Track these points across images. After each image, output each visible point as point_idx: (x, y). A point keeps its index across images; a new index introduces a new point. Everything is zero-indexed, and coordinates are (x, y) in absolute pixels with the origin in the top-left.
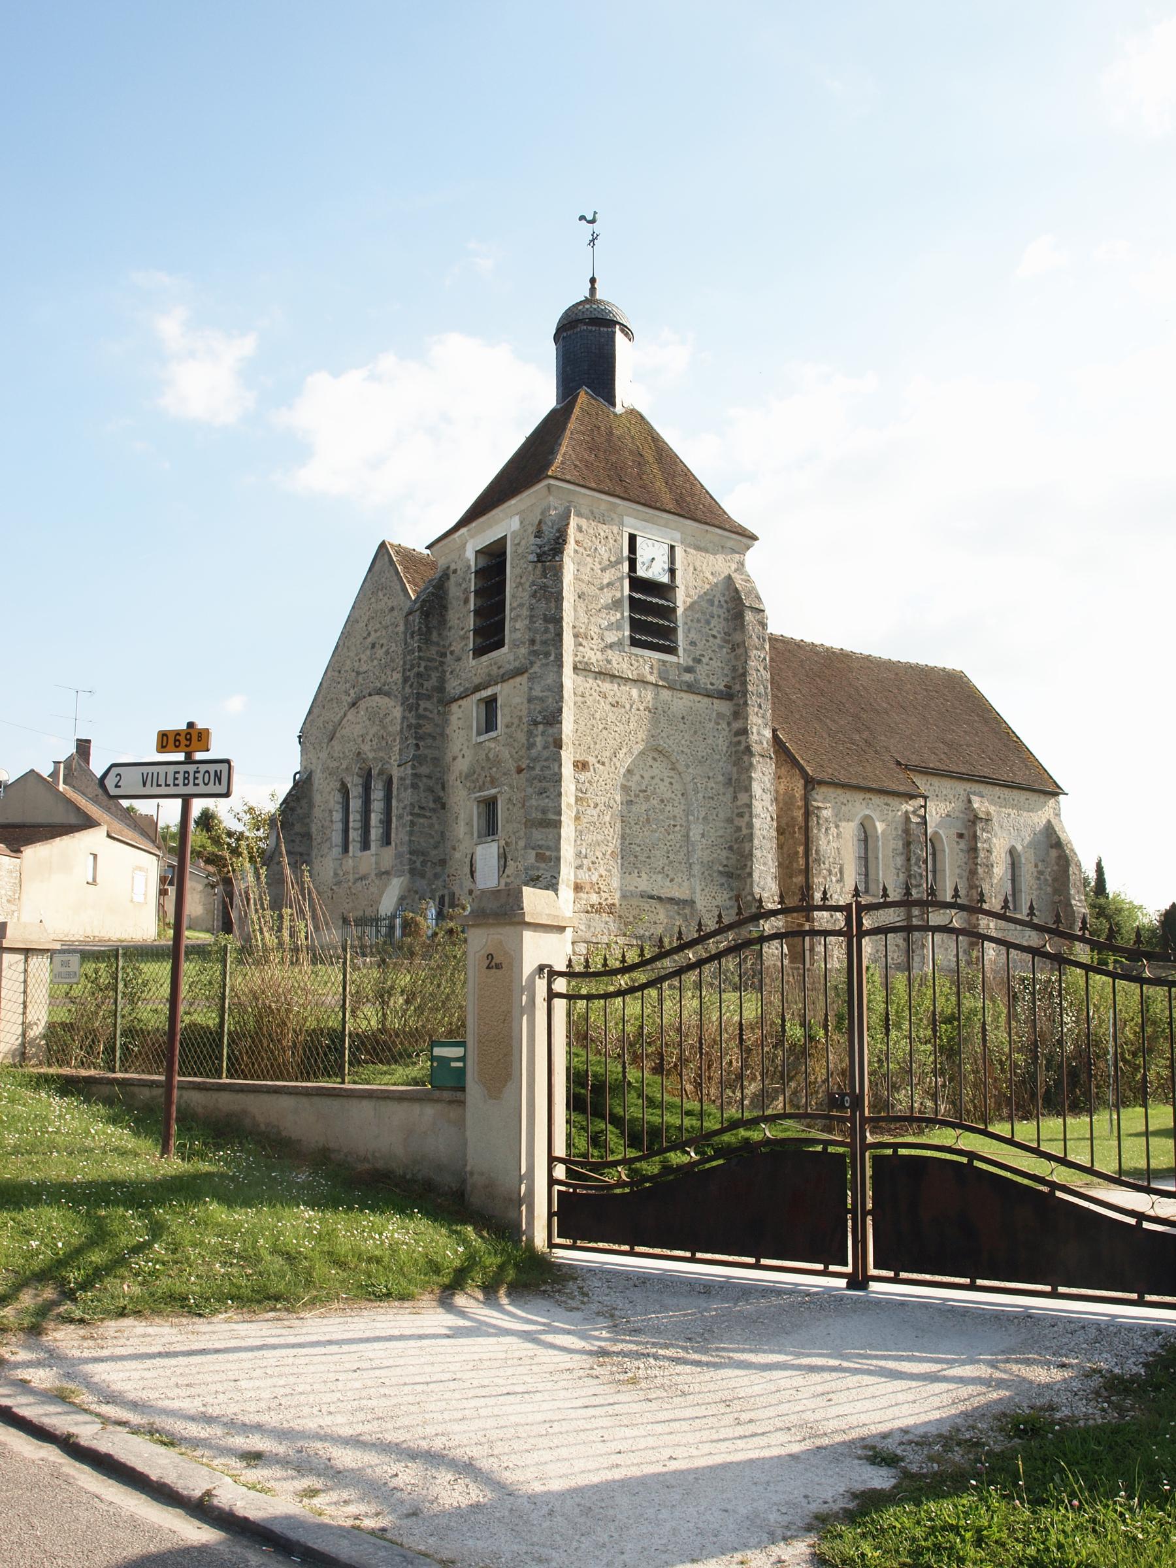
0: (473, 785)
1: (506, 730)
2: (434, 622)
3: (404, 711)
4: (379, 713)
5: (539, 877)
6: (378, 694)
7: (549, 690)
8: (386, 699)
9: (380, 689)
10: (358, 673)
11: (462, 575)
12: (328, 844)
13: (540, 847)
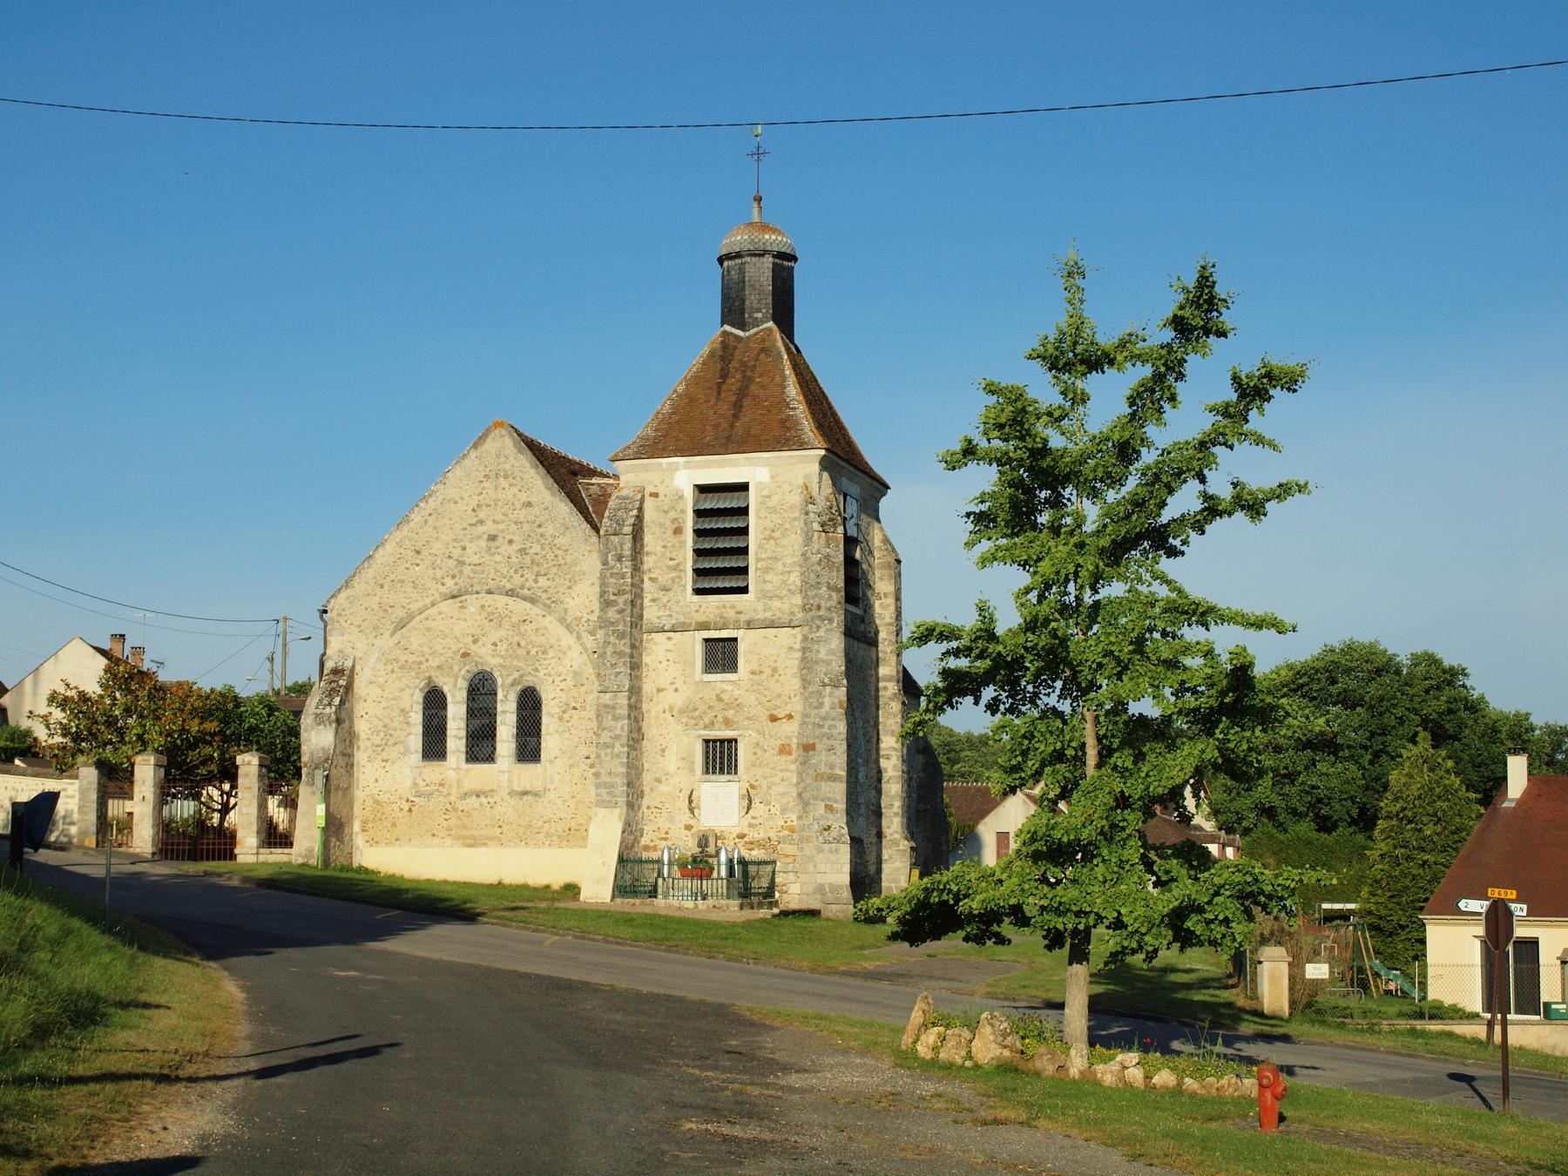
0: (693, 722)
1: (753, 676)
2: (639, 546)
3: (607, 635)
5: (829, 827)
6: (507, 594)
7: (834, 654)
8: (528, 605)
9: (511, 590)
10: (461, 563)
12: (400, 748)
13: (829, 799)
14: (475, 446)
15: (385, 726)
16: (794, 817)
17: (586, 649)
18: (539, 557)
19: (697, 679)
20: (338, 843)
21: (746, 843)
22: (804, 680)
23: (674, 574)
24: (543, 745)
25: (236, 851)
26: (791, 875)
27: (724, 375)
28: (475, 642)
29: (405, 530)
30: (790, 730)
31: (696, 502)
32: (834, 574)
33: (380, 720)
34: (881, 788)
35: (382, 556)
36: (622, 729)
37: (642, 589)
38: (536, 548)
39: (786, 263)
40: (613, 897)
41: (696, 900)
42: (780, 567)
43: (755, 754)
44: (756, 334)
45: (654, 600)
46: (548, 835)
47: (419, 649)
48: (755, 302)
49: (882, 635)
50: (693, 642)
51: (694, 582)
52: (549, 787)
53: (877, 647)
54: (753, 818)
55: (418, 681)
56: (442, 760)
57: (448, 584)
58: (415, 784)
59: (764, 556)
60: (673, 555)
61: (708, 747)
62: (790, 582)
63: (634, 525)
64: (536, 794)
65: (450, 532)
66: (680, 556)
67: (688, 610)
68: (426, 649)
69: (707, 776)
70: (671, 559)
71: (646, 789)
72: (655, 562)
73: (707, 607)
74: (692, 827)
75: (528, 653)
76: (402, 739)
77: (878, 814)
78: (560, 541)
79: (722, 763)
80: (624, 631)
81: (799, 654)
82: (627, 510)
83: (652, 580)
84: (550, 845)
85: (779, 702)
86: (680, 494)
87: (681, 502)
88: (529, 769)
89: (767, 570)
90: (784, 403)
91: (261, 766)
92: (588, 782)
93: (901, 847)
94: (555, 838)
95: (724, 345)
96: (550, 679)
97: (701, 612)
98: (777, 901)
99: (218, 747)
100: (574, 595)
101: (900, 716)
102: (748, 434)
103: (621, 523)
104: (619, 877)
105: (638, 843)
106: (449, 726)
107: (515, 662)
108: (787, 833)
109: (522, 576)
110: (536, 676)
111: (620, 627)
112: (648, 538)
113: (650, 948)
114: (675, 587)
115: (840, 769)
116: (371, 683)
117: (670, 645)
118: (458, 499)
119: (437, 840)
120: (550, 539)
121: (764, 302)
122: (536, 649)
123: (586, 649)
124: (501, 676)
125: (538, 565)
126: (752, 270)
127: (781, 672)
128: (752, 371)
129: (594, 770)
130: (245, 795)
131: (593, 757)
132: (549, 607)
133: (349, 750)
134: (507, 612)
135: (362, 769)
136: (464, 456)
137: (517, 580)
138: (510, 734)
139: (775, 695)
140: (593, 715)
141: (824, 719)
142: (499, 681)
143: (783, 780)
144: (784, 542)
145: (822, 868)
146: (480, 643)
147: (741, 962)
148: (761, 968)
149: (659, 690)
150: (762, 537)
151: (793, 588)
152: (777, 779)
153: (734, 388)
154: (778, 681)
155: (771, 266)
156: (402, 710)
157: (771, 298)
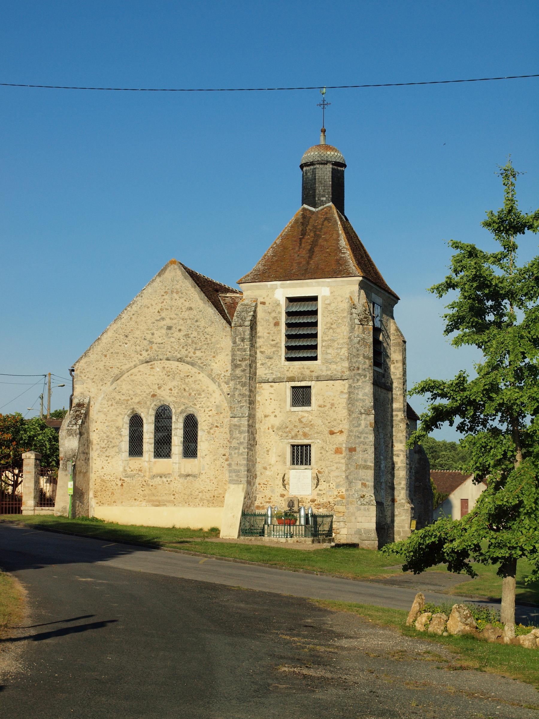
0: (285, 435)
3: (236, 384)
4: (180, 374)
5: (364, 496)
6: (178, 361)
7: (367, 396)
8: (190, 367)
9: (180, 358)
10: (151, 342)
11: (270, 307)
12: (116, 449)
14: (159, 275)
15: (107, 437)
16: (344, 490)
17: (223, 392)
18: (196, 339)
19: (288, 410)
20: (80, 504)
21: (316, 505)
22: (350, 410)
23: (274, 349)
24: (199, 448)
25: (22, 508)
26: (342, 524)
27: (304, 233)
28: (159, 388)
29: (119, 324)
30: (341, 439)
31: (287, 307)
32: (367, 349)
34: (394, 473)
35: (106, 338)
36: (244, 439)
37: (256, 358)
38: (195, 334)
39: (339, 168)
40: (239, 536)
41: (287, 537)
42: (335, 345)
43: (321, 453)
44: (323, 209)
45: (262, 364)
46: (202, 499)
47: (127, 392)
48: (322, 191)
49: (395, 385)
50: (286, 388)
51: (286, 353)
53: (392, 391)
54: (320, 490)
55: (126, 411)
56: (140, 456)
58: (125, 470)
59: (326, 339)
60: (274, 338)
61: (294, 449)
63: (251, 320)
64: (195, 476)
65: (145, 325)
66: (277, 339)
67: (283, 370)
68: (131, 392)
69: (293, 466)
70: (273, 340)
71: (258, 473)
74: (285, 495)
75: (190, 394)
76: (118, 444)
77: (392, 488)
78: (209, 330)
79: (302, 459)
80: (246, 382)
82: (247, 312)
83: (262, 352)
84: (202, 505)
85: (335, 423)
86: (278, 303)
87: (279, 307)
89: (328, 347)
90: (338, 250)
91: (36, 459)
93: (406, 508)
94: (205, 501)
95: (304, 216)
96: (203, 410)
98: (334, 539)
99: (13, 449)
100: (217, 361)
101: (405, 431)
102: (317, 268)
103: (243, 319)
104: (242, 524)
105: (254, 504)
107: (183, 400)
108: (339, 499)
109: (186, 350)
110: (195, 409)
111: (243, 380)
112: (260, 328)
113: (260, 565)
114: (275, 357)
115: (371, 462)
116: (99, 412)
117: (272, 390)
118: (149, 305)
119: (137, 503)
120: (203, 329)
121: (327, 191)
122: (195, 392)
123: (223, 392)
124: (175, 407)
125: (196, 344)
128: (320, 231)
129: (228, 462)
130: (27, 476)
131: (227, 454)
132: (202, 368)
133: (87, 451)
134: (178, 371)
135: (95, 462)
136: (153, 281)
137: (184, 352)
138: (180, 442)
139: (332, 419)
140: (227, 430)
141: (361, 433)
142: (173, 411)
143: (337, 468)
144: (338, 330)
145: (359, 519)
146: (162, 389)
147: (313, 573)
148: (324, 577)
150: (325, 327)
151: (343, 357)
152: (334, 468)
153: (309, 241)
154: (334, 411)
155: (331, 170)
156: (117, 428)
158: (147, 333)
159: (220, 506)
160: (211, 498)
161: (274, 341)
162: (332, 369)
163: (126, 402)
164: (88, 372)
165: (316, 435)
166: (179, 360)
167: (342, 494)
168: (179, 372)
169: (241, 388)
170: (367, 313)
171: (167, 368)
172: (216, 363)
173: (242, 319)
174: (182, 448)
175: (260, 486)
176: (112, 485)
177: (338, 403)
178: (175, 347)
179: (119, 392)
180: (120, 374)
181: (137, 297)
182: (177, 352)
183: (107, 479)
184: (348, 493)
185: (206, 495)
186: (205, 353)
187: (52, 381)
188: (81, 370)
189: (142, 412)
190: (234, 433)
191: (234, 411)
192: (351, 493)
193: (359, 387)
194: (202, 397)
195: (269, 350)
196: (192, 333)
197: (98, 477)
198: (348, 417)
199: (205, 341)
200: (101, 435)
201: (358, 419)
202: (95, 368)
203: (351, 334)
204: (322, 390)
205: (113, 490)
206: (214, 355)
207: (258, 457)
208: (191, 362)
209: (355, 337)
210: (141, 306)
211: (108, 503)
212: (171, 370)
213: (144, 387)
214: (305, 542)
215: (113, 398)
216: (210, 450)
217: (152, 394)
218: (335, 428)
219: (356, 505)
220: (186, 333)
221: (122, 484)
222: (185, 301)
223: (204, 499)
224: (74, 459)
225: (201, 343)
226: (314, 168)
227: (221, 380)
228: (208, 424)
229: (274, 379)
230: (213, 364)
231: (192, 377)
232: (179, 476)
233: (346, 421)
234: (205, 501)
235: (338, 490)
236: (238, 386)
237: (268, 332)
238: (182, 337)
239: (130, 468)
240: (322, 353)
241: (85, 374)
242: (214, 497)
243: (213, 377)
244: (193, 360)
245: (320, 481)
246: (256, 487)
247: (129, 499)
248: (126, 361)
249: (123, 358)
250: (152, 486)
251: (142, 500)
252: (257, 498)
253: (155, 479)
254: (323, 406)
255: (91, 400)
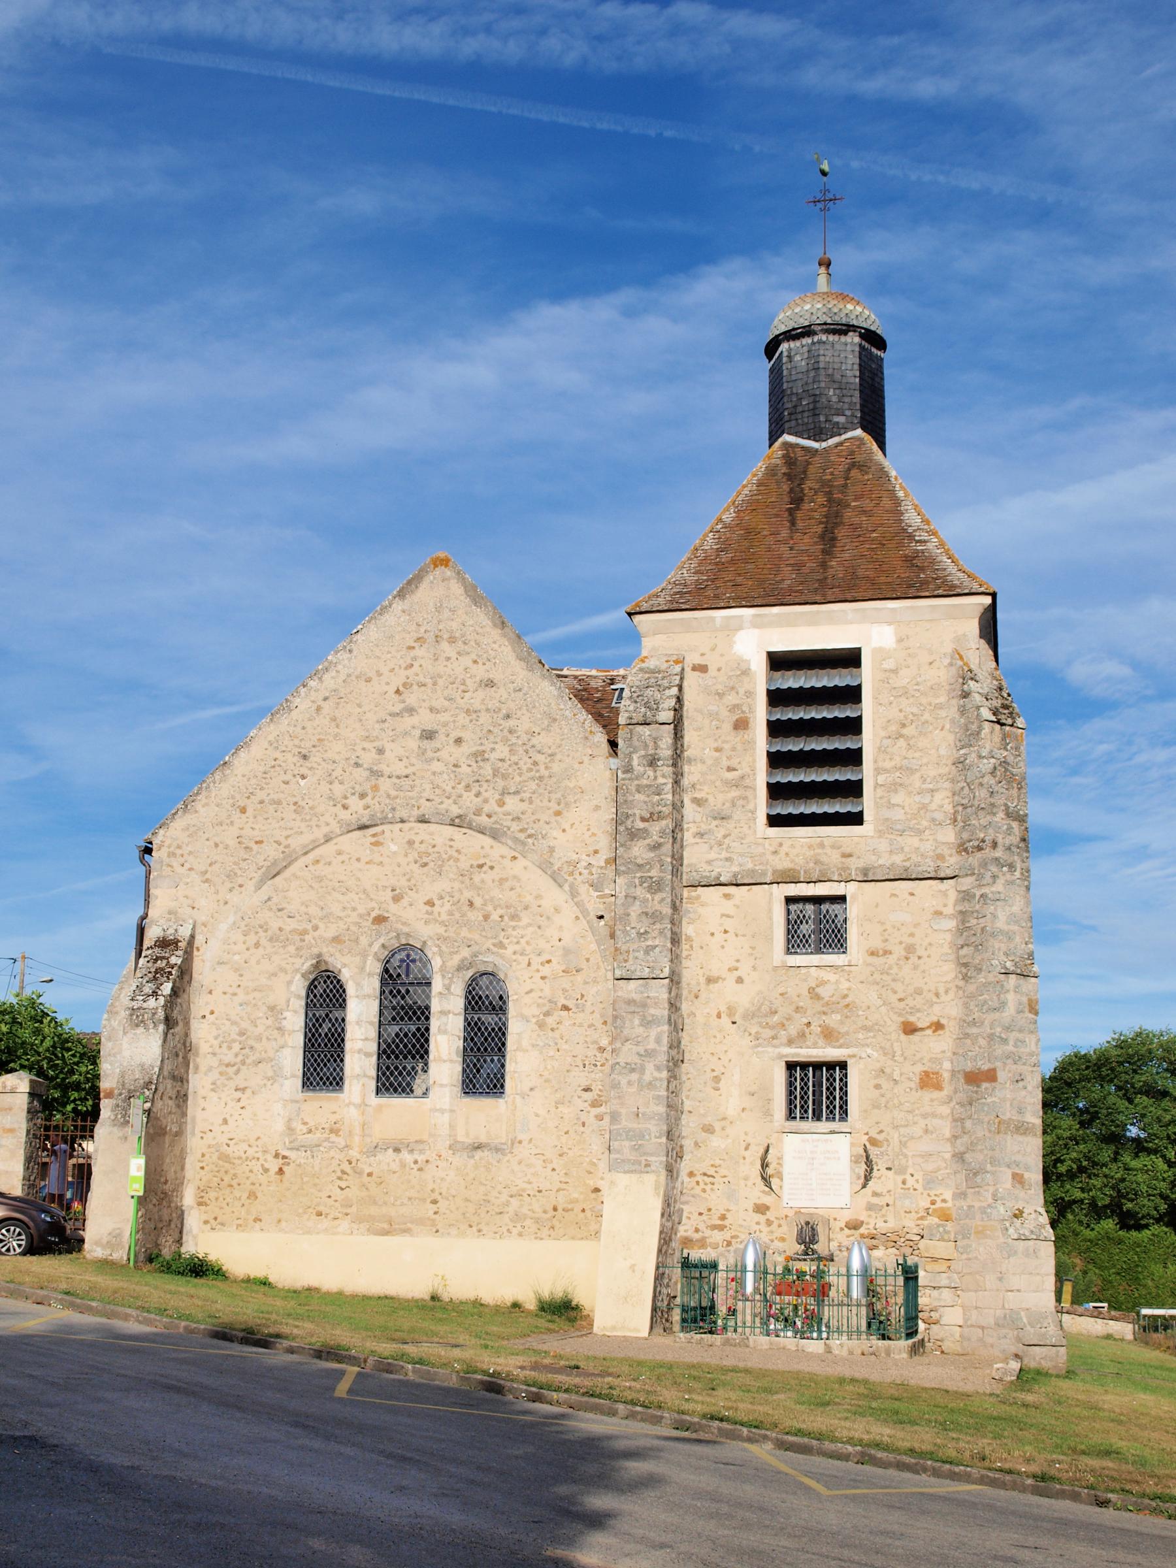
0: (768, 1033)
7: (1017, 922)
8: (487, 841)
9: (459, 817)
10: (376, 773)
14: (401, 594)
15: (242, 1034)
16: (948, 1195)
17: (585, 912)
18: (506, 765)
21: (862, 1236)
23: (734, 793)
24: (509, 1067)
27: (797, 500)
28: (397, 899)
29: (284, 722)
33: (234, 1023)
35: (245, 763)
36: (658, 1041)
38: (502, 751)
39: (874, 350)
43: (877, 1087)
44: (841, 444)
45: (701, 835)
46: (518, 1217)
47: (303, 909)
48: (834, 399)
50: (770, 902)
52: (520, 1137)
54: (875, 1194)
55: (299, 961)
56: (334, 1090)
57: (353, 808)
58: (290, 1130)
59: (888, 765)
60: (734, 763)
62: (933, 806)
67: (760, 850)
68: (313, 910)
70: (730, 769)
72: (703, 774)
73: (792, 846)
74: (768, 1208)
75: (486, 917)
76: (271, 1054)
79: (817, 1103)
80: (662, 879)
81: (952, 924)
82: (661, 689)
83: (698, 802)
84: (520, 1235)
85: (918, 1001)
86: (743, 666)
87: (746, 679)
88: (485, 1104)
89: (894, 787)
91: (32, 1094)
92: (587, 1130)
94: (528, 1222)
97: (782, 854)
100: (567, 827)
106: (348, 1036)
107: (464, 933)
109: (478, 795)
110: (502, 957)
111: (653, 873)
112: (690, 736)
114: (737, 815)
116: (219, 963)
117: (728, 907)
118: (372, 674)
119: (325, 1223)
120: (525, 738)
122: (500, 912)
123: (585, 912)
124: (441, 954)
125: (505, 777)
126: (829, 353)
127: (920, 952)
132: (524, 844)
135: (201, 1101)
136: (384, 610)
137: (469, 801)
139: (911, 989)
141: (1008, 1029)
142: (436, 963)
143: (926, 1131)
149: (710, 980)
150: (883, 734)
151: (939, 816)
152: (917, 1130)
153: (817, 515)
154: (915, 968)
155: (857, 349)
156: (272, 1008)
157: (857, 394)
158: (364, 749)
159: (573, 1238)
160: (545, 1212)
161: (735, 770)
162: (906, 849)
163: (297, 938)
164: (190, 853)
165: (860, 1036)
166: (457, 821)
167: (944, 1205)
168: (456, 854)
169: (649, 896)
170: (1005, 695)
171: (422, 842)
172: (564, 831)
173: (647, 705)
174: (460, 1069)
175: (695, 1179)
176: (251, 1171)
177: (925, 944)
178: (444, 786)
179: (280, 910)
180: (284, 859)
181: (337, 652)
182: (450, 801)
183: (237, 1154)
184: (964, 1204)
185: (530, 1204)
186: (531, 803)
187: (27, 971)
188: (172, 849)
189: (345, 965)
190: (628, 1024)
191: (626, 961)
192: (977, 1204)
193: (997, 896)
194: (520, 924)
195: (721, 797)
196: (493, 749)
197: (209, 1147)
198: (961, 983)
199: (530, 770)
200: (222, 1027)
201: (998, 988)
202: (211, 843)
203: (962, 752)
204: (877, 906)
205: (253, 1184)
206: (558, 808)
207: (687, 1097)
208: (491, 828)
209: (980, 757)
210: (349, 675)
211: (239, 1222)
212: (431, 850)
213: (352, 895)
214: (888, 1354)
215: (261, 927)
216: (546, 1073)
217: (374, 914)
218: (918, 1015)
219: (1002, 1240)
220: (474, 749)
221: (281, 1169)
222: (475, 662)
223: (525, 1217)
224: (147, 1093)
225: (520, 775)
226: (813, 343)
227: (580, 879)
228: (540, 1001)
229: (735, 875)
230: (556, 833)
231: (492, 868)
232: (450, 1147)
233: (951, 995)
234: (528, 1222)
235: (932, 1193)
236: (639, 889)
237: (716, 745)
238: (463, 759)
239: (305, 1123)
240: (876, 803)
241: (182, 860)
242: (555, 1209)
243: (556, 868)
244: (496, 822)
245: (875, 1168)
246: (683, 1183)
247: (301, 1211)
248: (303, 825)
249: (294, 816)
250: (370, 1175)
251: (340, 1215)
252: (685, 1214)
253: (380, 1157)
254: (881, 952)
255: (198, 931)
